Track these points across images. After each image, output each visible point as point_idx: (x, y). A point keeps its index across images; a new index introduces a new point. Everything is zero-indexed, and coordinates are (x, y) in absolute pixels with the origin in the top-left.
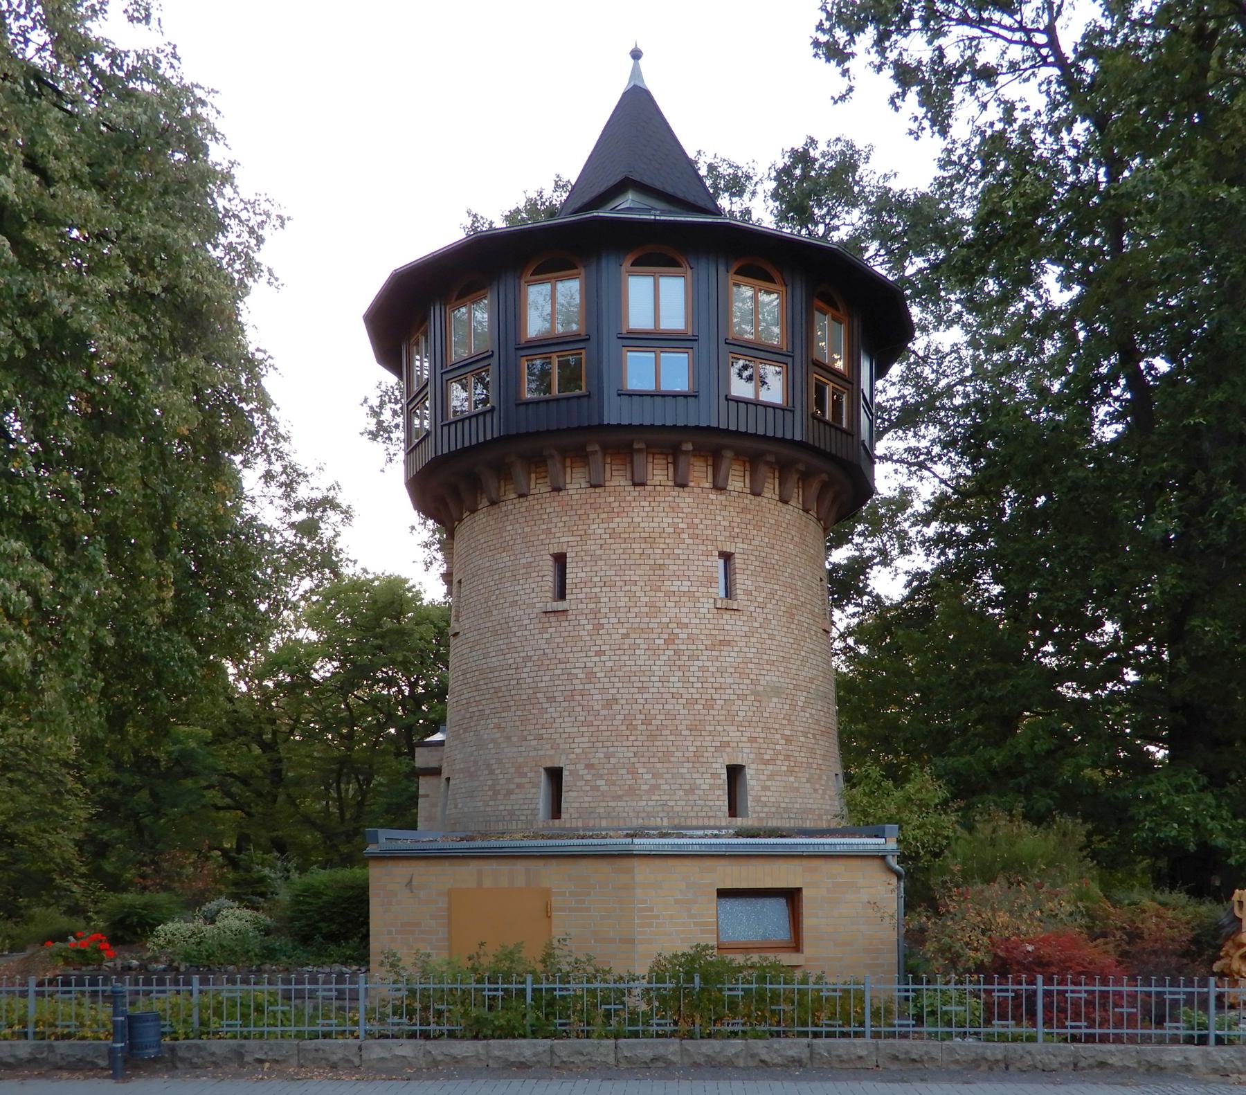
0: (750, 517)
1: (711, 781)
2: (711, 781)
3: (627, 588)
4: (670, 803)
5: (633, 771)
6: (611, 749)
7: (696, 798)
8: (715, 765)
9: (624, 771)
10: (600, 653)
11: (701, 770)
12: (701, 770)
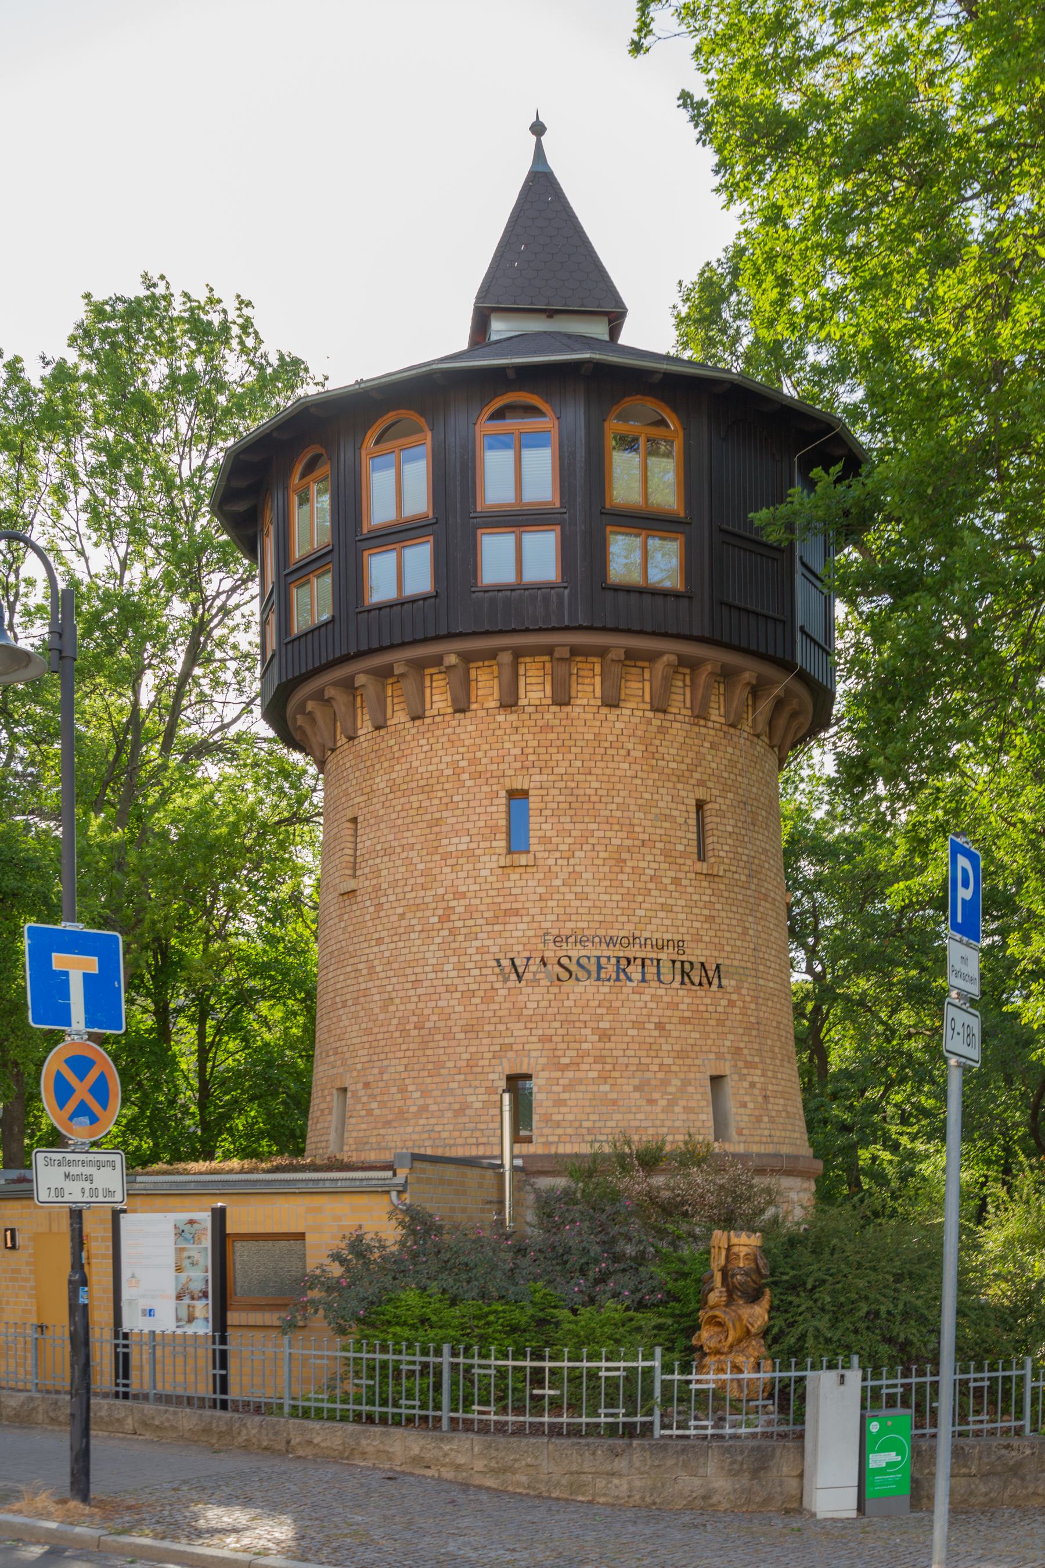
0: (553, 736)
1: (485, 1097)
2: (485, 1097)
3: (405, 855)
4: (438, 1128)
5: (403, 1090)
6: (385, 1063)
7: (466, 1119)
8: (491, 1076)
9: (394, 1090)
10: (380, 941)
11: (474, 1083)
12: (474, 1083)
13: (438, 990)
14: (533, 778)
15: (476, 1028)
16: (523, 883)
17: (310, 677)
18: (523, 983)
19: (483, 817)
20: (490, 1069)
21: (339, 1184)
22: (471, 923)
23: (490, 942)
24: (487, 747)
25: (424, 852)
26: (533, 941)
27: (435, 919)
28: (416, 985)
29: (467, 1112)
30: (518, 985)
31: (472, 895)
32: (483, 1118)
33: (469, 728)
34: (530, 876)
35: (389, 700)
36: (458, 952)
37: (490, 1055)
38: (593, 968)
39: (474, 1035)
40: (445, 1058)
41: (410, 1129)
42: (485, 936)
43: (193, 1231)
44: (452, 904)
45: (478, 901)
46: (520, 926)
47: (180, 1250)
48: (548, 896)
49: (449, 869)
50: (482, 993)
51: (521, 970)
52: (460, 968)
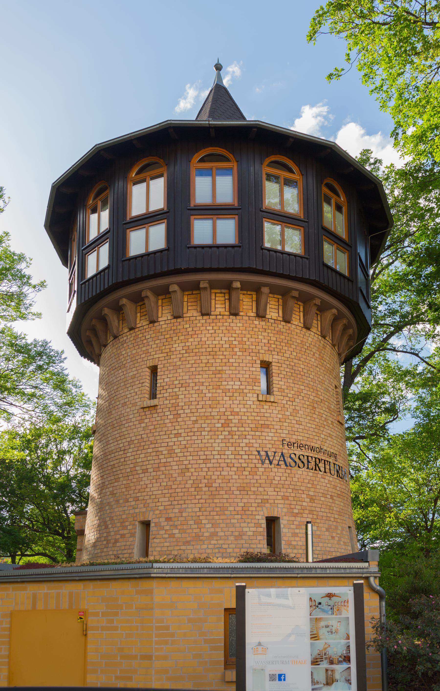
0: (283, 337)
1: (254, 529)
2: (254, 529)
3: (197, 388)
4: (224, 546)
5: (198, 522)
6: (184, 506)
7: (243, 542)
8: (257, 517)
9: (192, 522)
10: (178, 435)
11: (247, 521)
12: (247, 521)
13: (222, 465)
14: (274, 356)
15: (246, 489)
16: (270, 411)
17: (134, 283)
18: (273, 466)
19: (248, 373)
20: (257, 513)
21: (328, 571)
22: (243, 429)
23: (254, 441)
24: (249, 336)
25: (211, 387)
26: (277, 443)
27: (220, 425)
28: (206, 461)
29: (244, 537)
30: (270, 466)
31: (242, 414)
32: (254, 542)
33: (238, 325)
34: (274, 408)
35: (185, 304)
36: (234, 445)
37: (256, 505)
38: (306, 462)
39: (245, 493)
40: (228, 505)
41: (205, 547)
42: (250, 437)
43: (331, 603)
44: (230, 417)
45: (246, 418)
46: (270, 434)
47: (315, 621)
48: (283, 420)
49: (228, 398)
50: (249, 469)
51: (271, 458)
52: (236, 454)
